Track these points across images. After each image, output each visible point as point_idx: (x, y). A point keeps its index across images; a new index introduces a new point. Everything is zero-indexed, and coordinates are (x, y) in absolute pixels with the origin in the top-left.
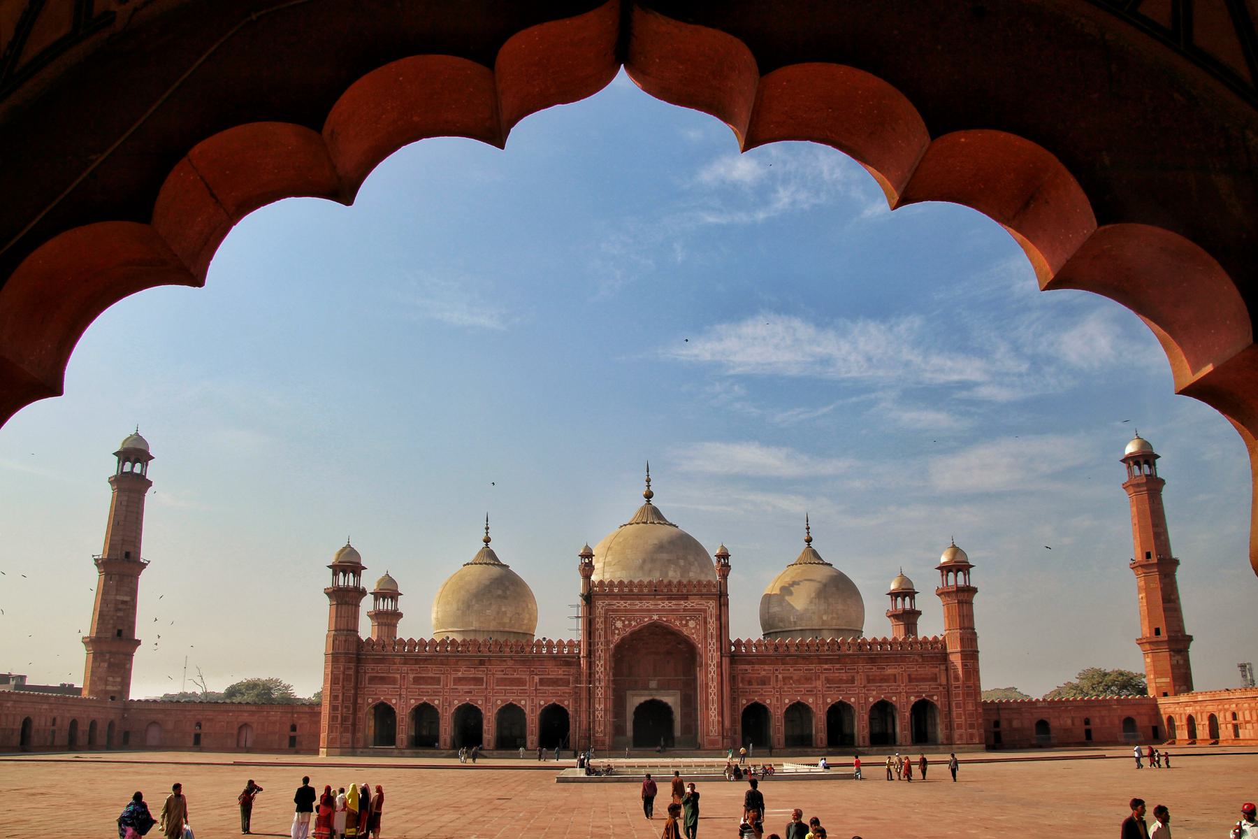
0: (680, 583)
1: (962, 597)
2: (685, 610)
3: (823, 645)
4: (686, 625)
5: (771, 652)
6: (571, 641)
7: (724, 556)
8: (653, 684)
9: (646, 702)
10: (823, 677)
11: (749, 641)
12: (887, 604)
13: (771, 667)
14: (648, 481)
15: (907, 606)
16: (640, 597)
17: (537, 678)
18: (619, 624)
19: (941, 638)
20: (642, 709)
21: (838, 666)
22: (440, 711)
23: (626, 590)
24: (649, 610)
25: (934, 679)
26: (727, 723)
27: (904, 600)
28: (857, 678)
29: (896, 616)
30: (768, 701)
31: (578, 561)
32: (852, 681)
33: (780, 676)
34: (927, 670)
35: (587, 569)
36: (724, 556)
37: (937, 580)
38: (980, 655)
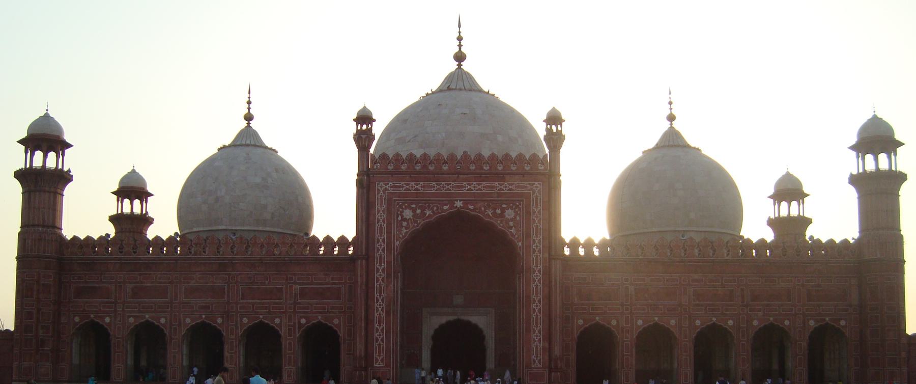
0: (493, 157)
2: (499, 195)
4: (502, 215)
6: (343, 239)
7: (554, 119)
8: (459, 300)
9: (449, 323)
14: (460, 39)
16: (437, 176)
17: (296, 287)
18: (408, 214)
20: (441, 334)
22: (166, 332)
23: (418, 167)
24: (449, 195)
26: (557, 351)
30: (614, 322)
31: (353, 128)
35: (363, 139)
36: (554, 119)
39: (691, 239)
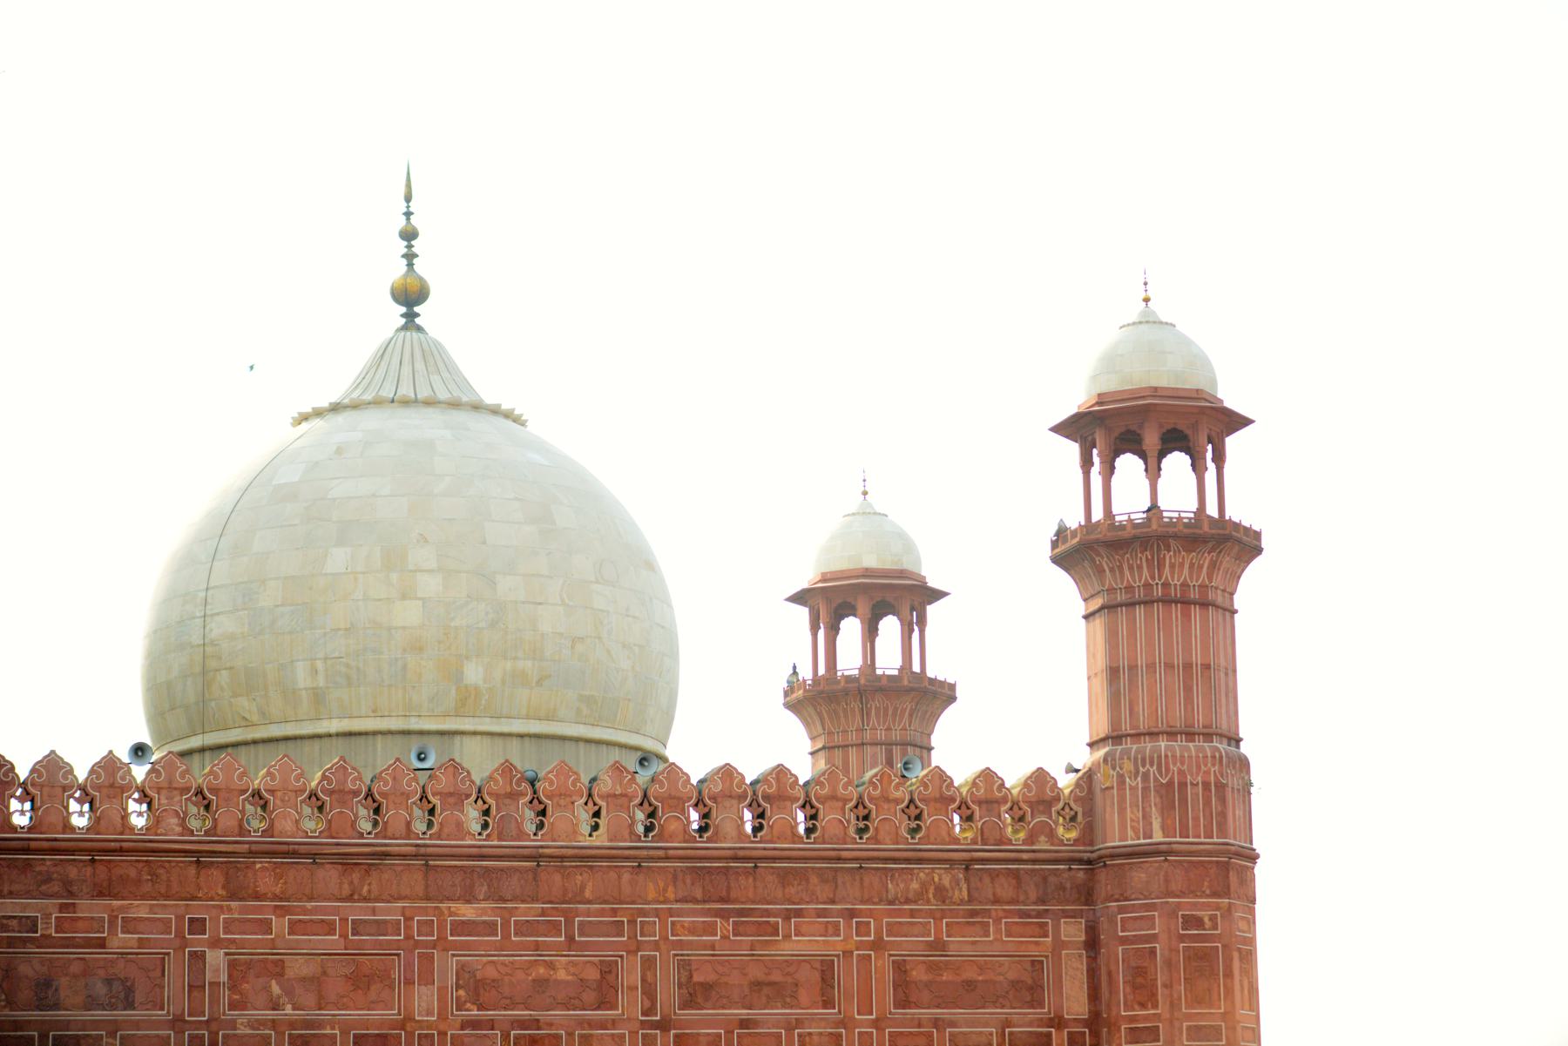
1: (1179, 571)
3: (457, 798)
5: (171, 830)
10: (447, 966)
11: (52, 768)
12: (792, 645)
13: (168, 912)
15: (889, 659)
19: (1065, 781)
21: (527, 911)
25: (1030, 991)
27: (871, 632)
28: (630, 974)
29: (819, 700)
32: (605, 990)
33: (216, 959)
34: (994, 944)
37: (1058, 489)
38: (1260, 870)
39: (454, 767)
